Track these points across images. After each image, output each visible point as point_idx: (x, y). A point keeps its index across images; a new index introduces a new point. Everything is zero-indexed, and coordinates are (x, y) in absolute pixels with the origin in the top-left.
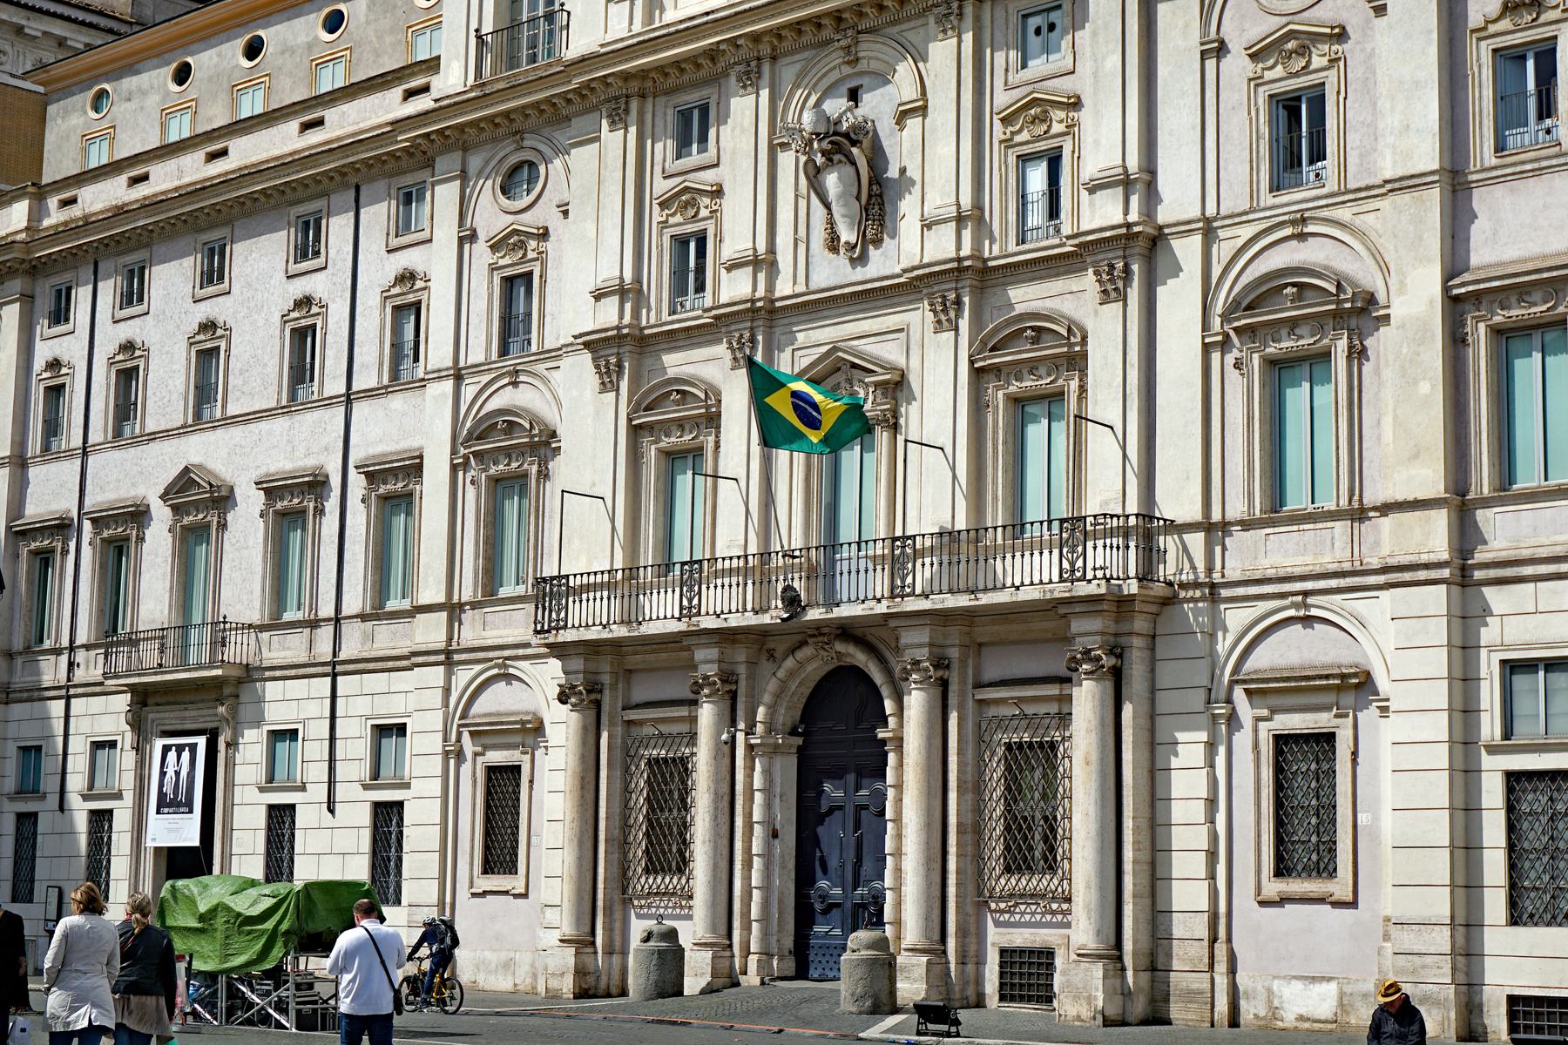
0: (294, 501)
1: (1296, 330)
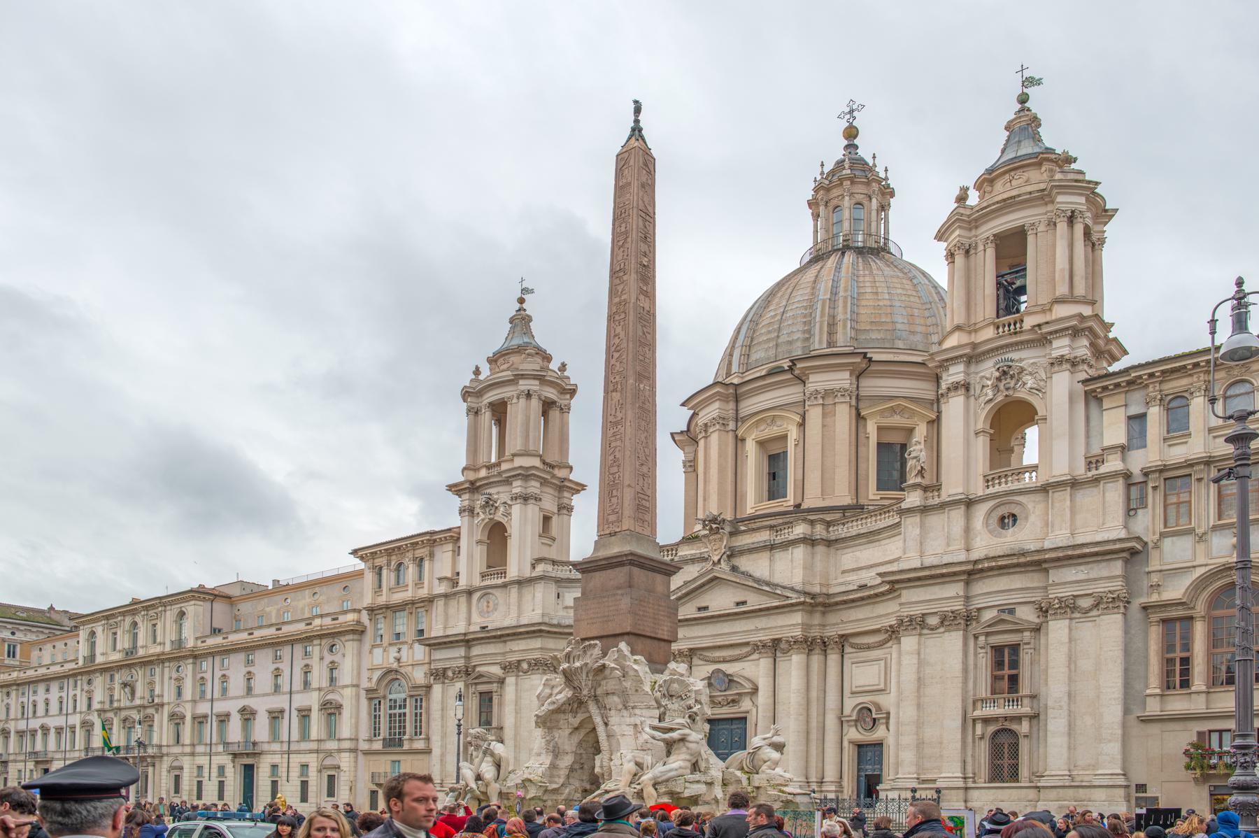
0: (59, 731)
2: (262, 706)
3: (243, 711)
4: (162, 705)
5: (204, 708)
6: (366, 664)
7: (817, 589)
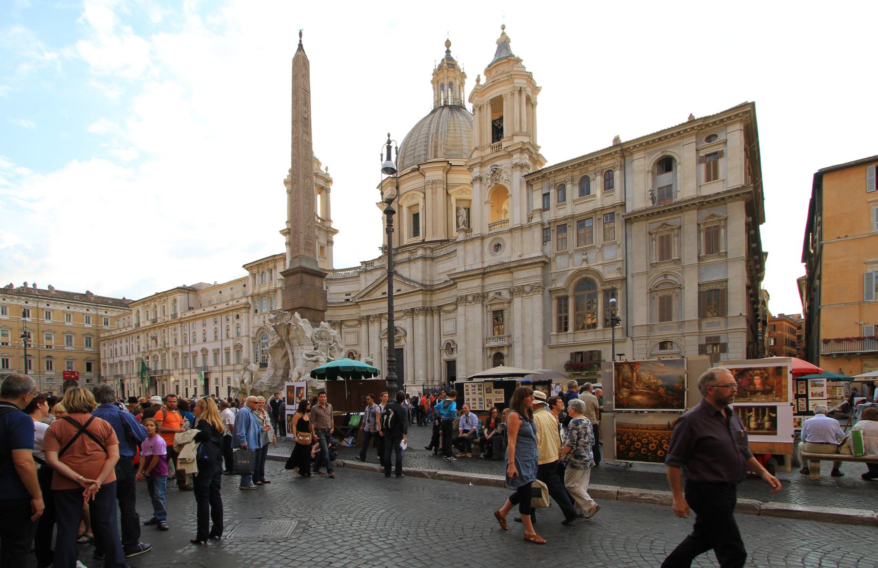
1: (175, 354)
2: (210, 347)
3: (202, 350)
4: (169, 348)
5: (186, 350)
6: (251, 325)
7: (428, 283)
